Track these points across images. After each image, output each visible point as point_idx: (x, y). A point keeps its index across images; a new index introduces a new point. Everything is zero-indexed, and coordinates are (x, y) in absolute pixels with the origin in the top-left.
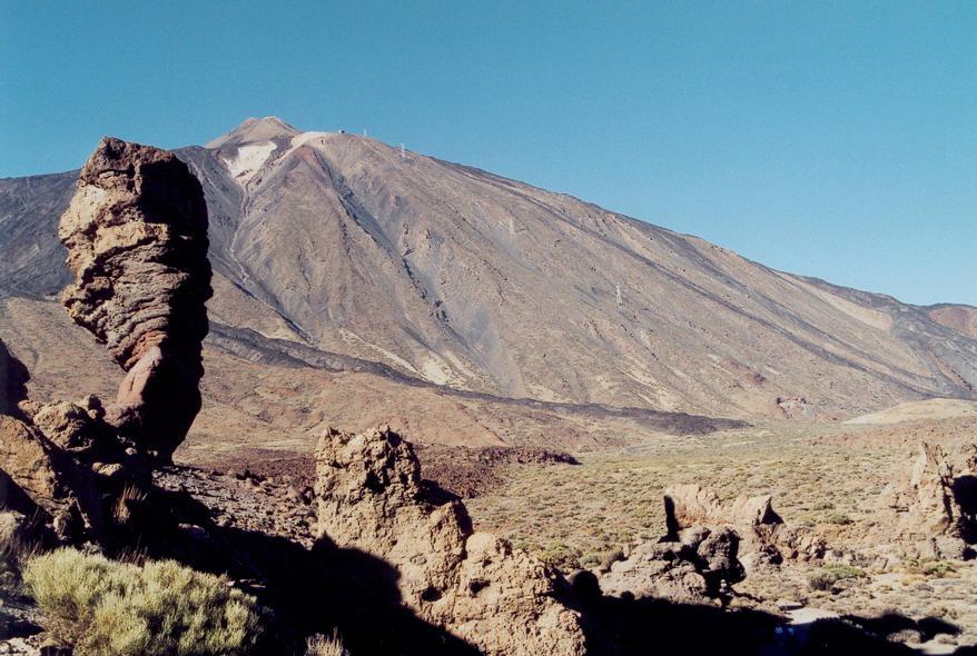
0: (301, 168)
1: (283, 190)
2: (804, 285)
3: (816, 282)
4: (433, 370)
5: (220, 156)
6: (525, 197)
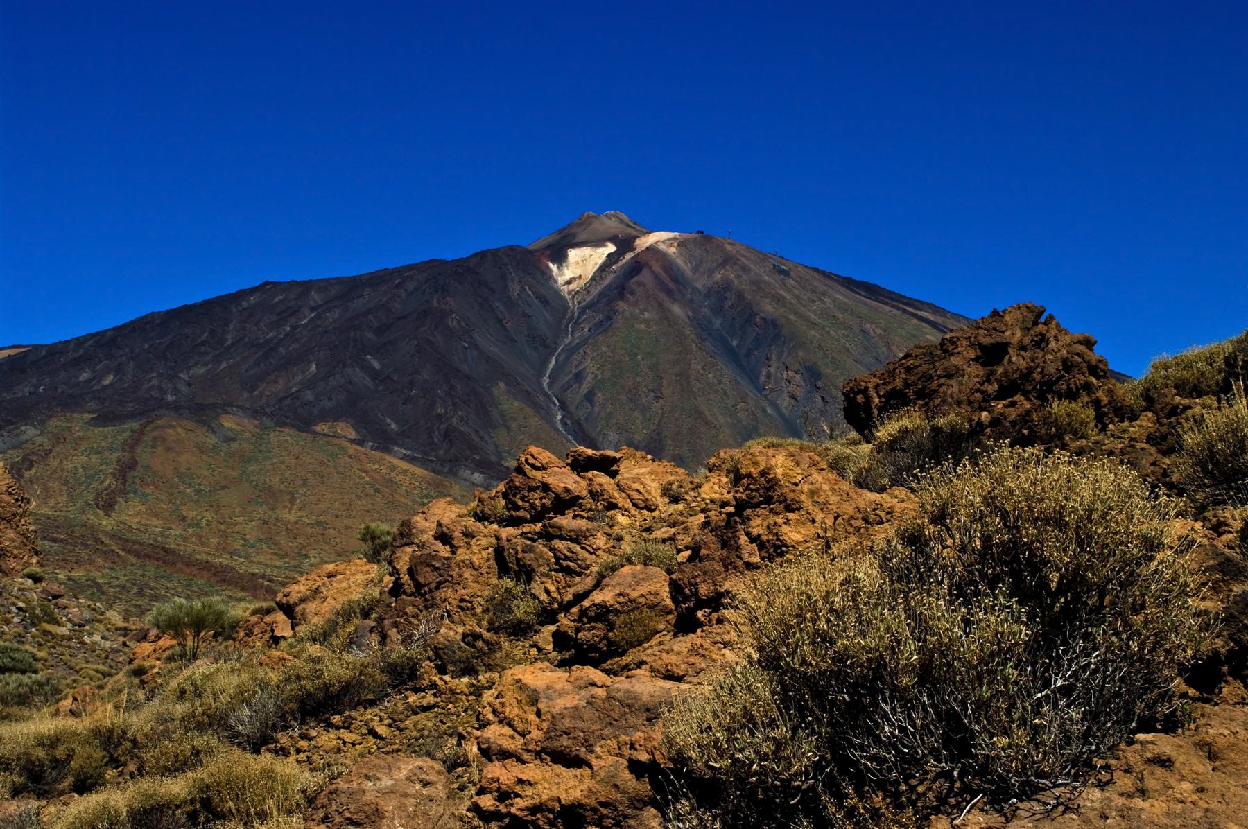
0: (645, 276)
1: (622, 305)
5: (544, 260)
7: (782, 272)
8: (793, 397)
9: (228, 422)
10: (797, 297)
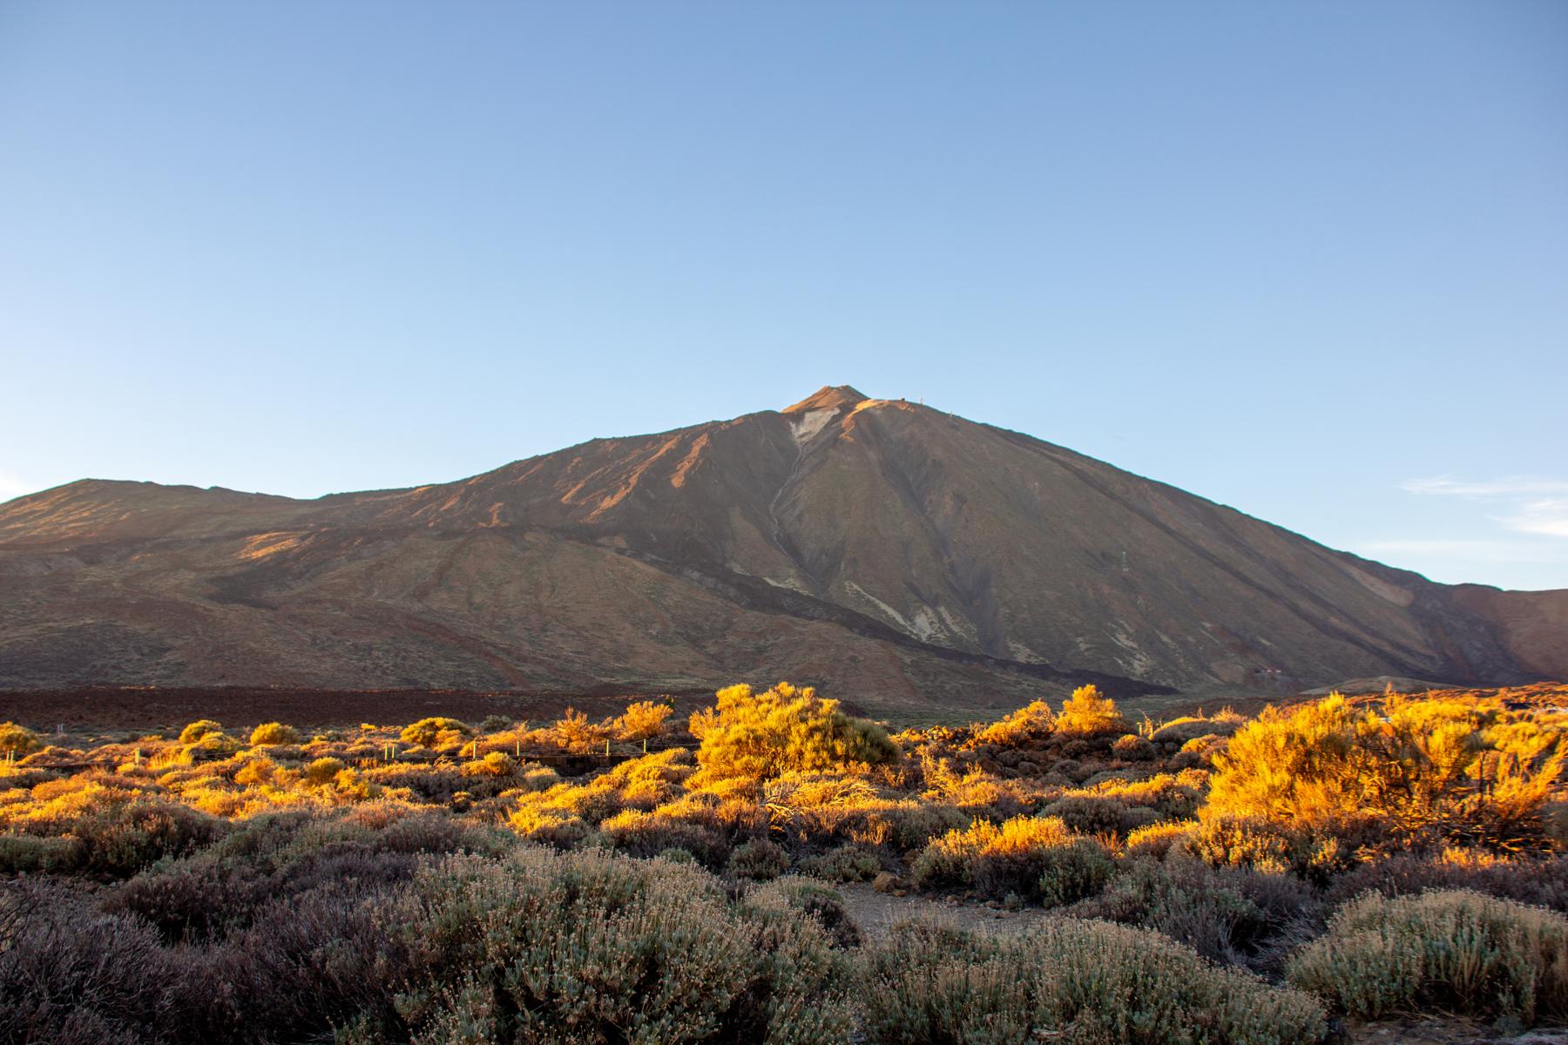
1: (832, 452)
3: (1349, 558)
4: (923, 625)
6: (1063, 464)
9: (530, 537)
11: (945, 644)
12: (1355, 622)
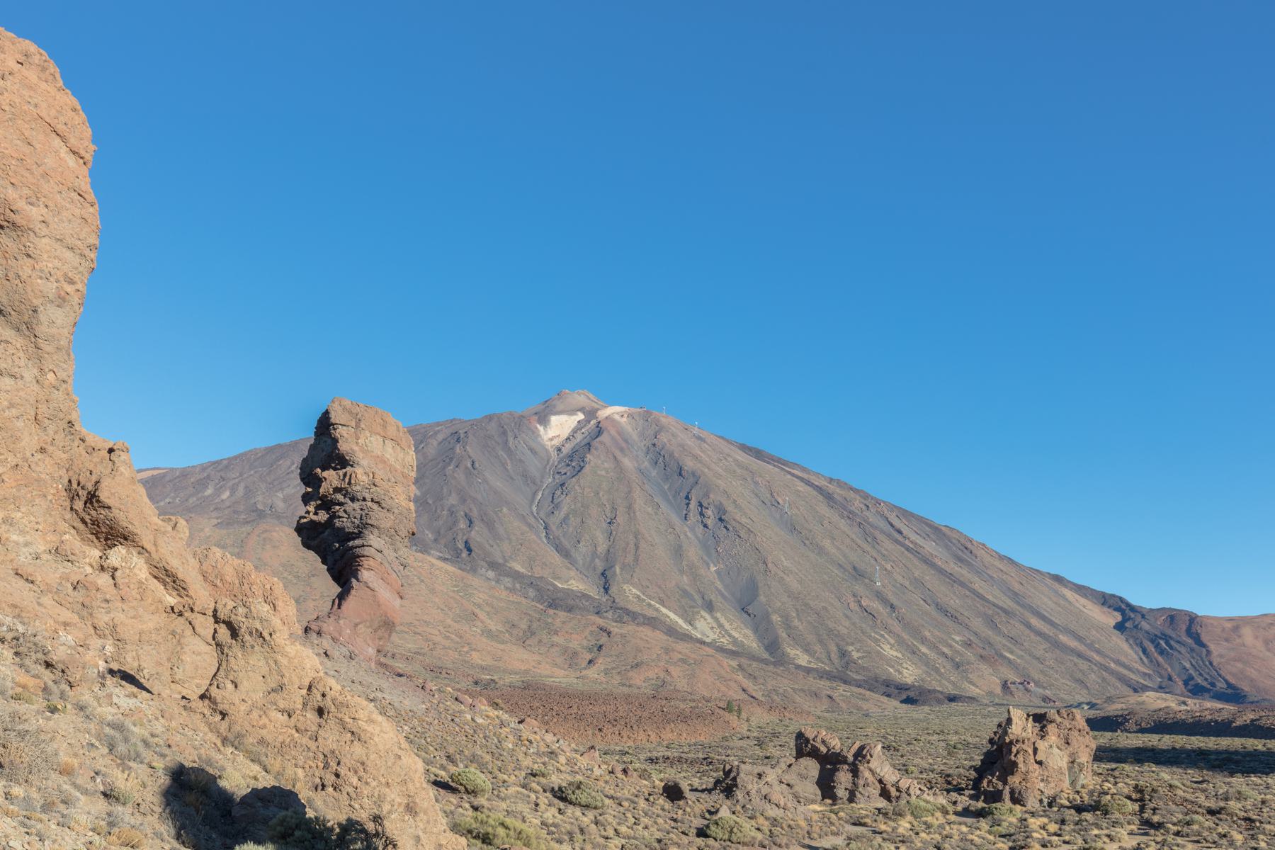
0: (604, 438)
2: (1048, 581)
4: (704, 627)
6: (802, 479)
7: (699, 438)
8: (705, 526)
10: (709, 457)
11: (730, 647)
12: (1080, 639)
